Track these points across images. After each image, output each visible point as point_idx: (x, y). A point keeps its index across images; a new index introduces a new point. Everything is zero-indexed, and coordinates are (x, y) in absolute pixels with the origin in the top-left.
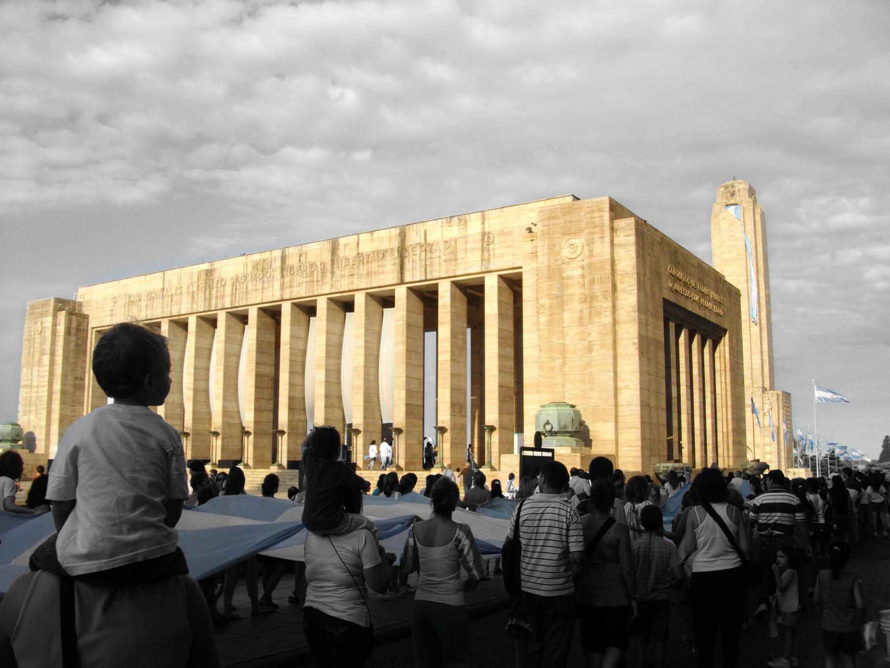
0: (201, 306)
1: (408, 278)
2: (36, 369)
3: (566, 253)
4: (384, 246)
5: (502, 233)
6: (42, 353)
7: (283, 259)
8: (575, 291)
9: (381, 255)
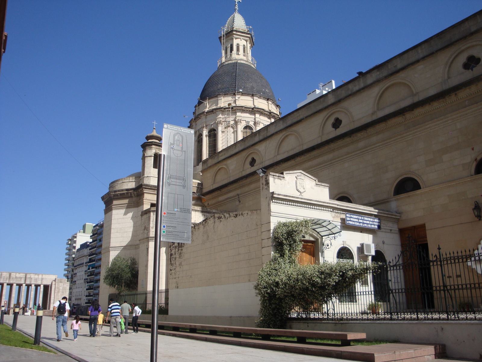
5: (45, 279)
9: (21, 278)
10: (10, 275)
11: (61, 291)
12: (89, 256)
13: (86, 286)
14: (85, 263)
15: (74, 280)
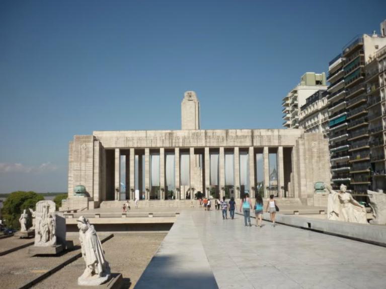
0: (167, 145)
1: (255, 144)
2: (83, 164)
3: (313, 145)
4: (246, 134)
5: (284, 136)
6: (88, 157)
7: (206, 133)
8: (315, 155)
10: (227, 133)
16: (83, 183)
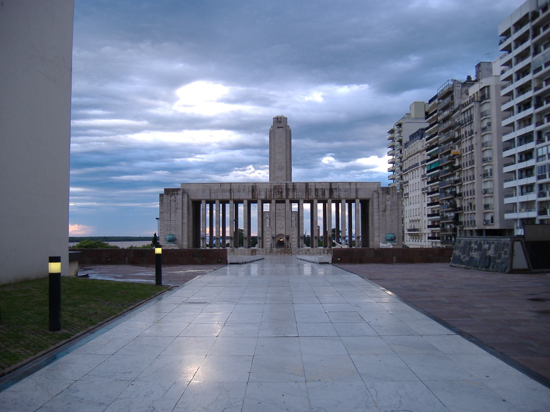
0: (250, 197)
2: (173, 215)
4: (324, 187)
11: (389, 207)
12: (427, 150)
13: (427, 199)
14: (420, 164)
15: (405, 192)
16: (173, 232)
